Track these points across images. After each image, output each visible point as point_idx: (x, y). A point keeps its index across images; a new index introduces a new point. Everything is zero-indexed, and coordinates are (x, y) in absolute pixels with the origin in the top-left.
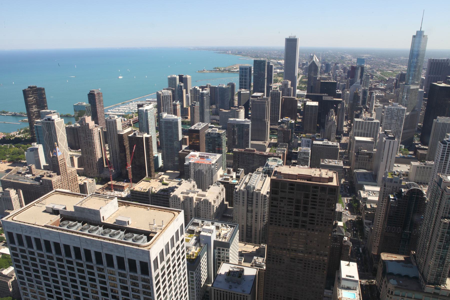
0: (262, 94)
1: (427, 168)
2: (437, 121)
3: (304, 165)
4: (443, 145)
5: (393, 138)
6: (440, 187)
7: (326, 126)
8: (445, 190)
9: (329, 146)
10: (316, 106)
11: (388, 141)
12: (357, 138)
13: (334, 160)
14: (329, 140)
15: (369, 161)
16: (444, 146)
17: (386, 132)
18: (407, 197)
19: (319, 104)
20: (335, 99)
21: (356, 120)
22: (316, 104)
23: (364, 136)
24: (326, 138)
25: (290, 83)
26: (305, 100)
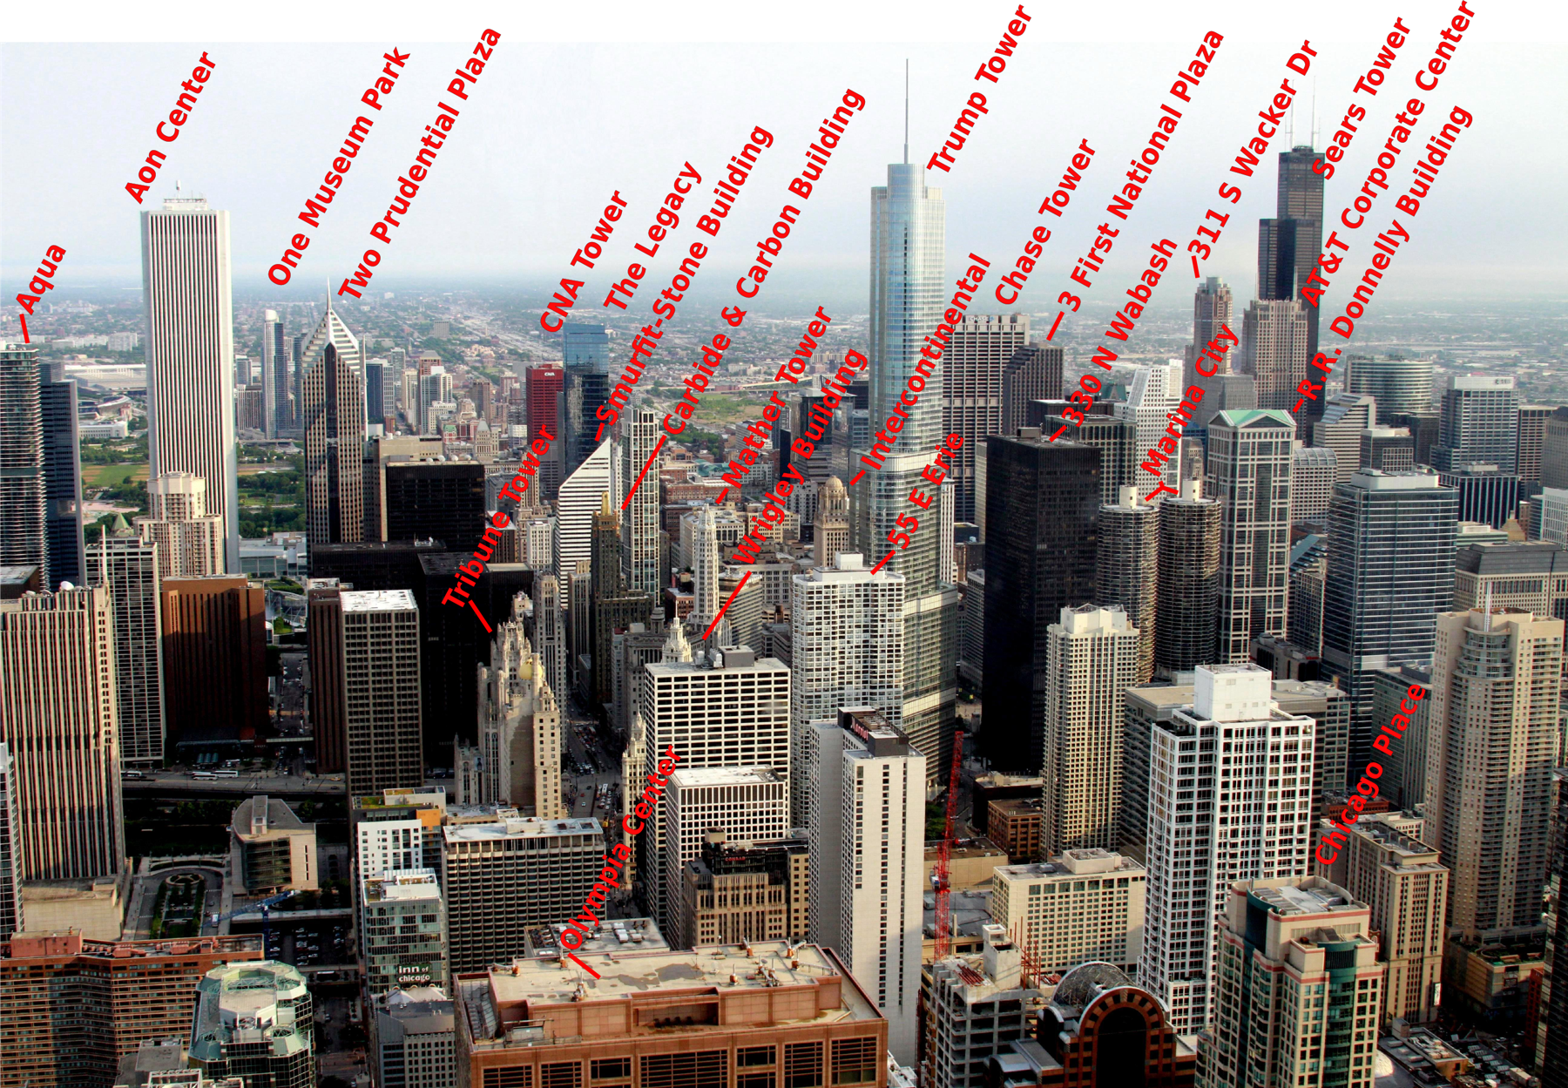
0: (30, 570)
1: (1080, 885)
2: (1067, 629)
3: (427, 984)
4: (1178, 740)
5: (901, 745)
6: (1262, 949)
7: (485, 728)
8: (1287, 959)
9: (543, 842)
10: (403, 616)
11: (873, 767)
12: (686, 778)
13: (606, 925)
14: (525, 803)
15: (775, 897)
16: (1184, 747)
17: (846, 721)
18: (1088, 1046)
19: (418, 598)
20: (494, 567)
21: (657, 670)
22: (397, 600)
23: (715, 762)
24: (504, 804)
25: (198, 486)
26: (312, 584)
